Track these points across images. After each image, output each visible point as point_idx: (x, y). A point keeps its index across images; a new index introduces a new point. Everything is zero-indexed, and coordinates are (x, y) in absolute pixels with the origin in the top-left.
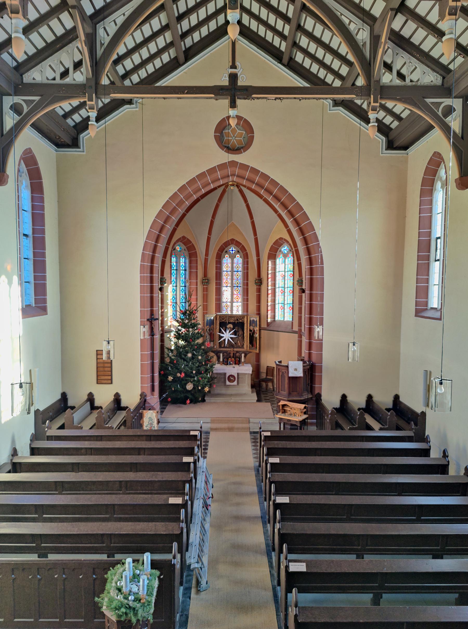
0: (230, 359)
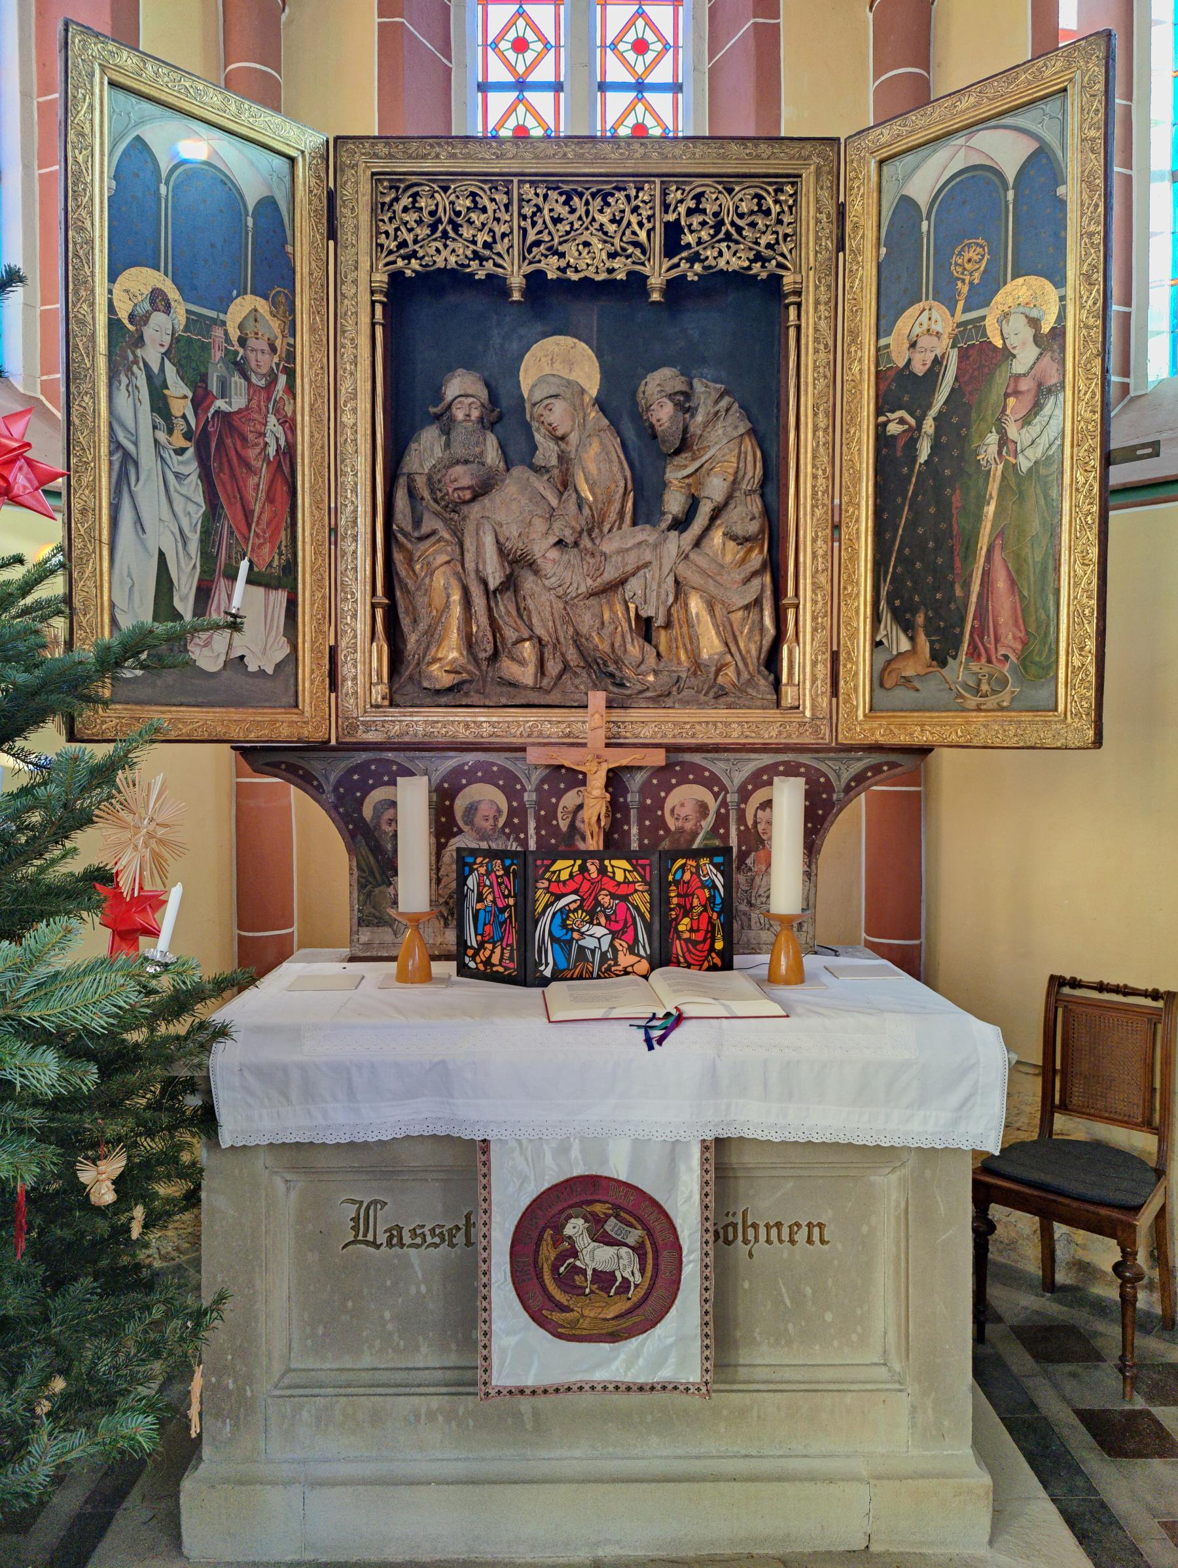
0: (564, 867)
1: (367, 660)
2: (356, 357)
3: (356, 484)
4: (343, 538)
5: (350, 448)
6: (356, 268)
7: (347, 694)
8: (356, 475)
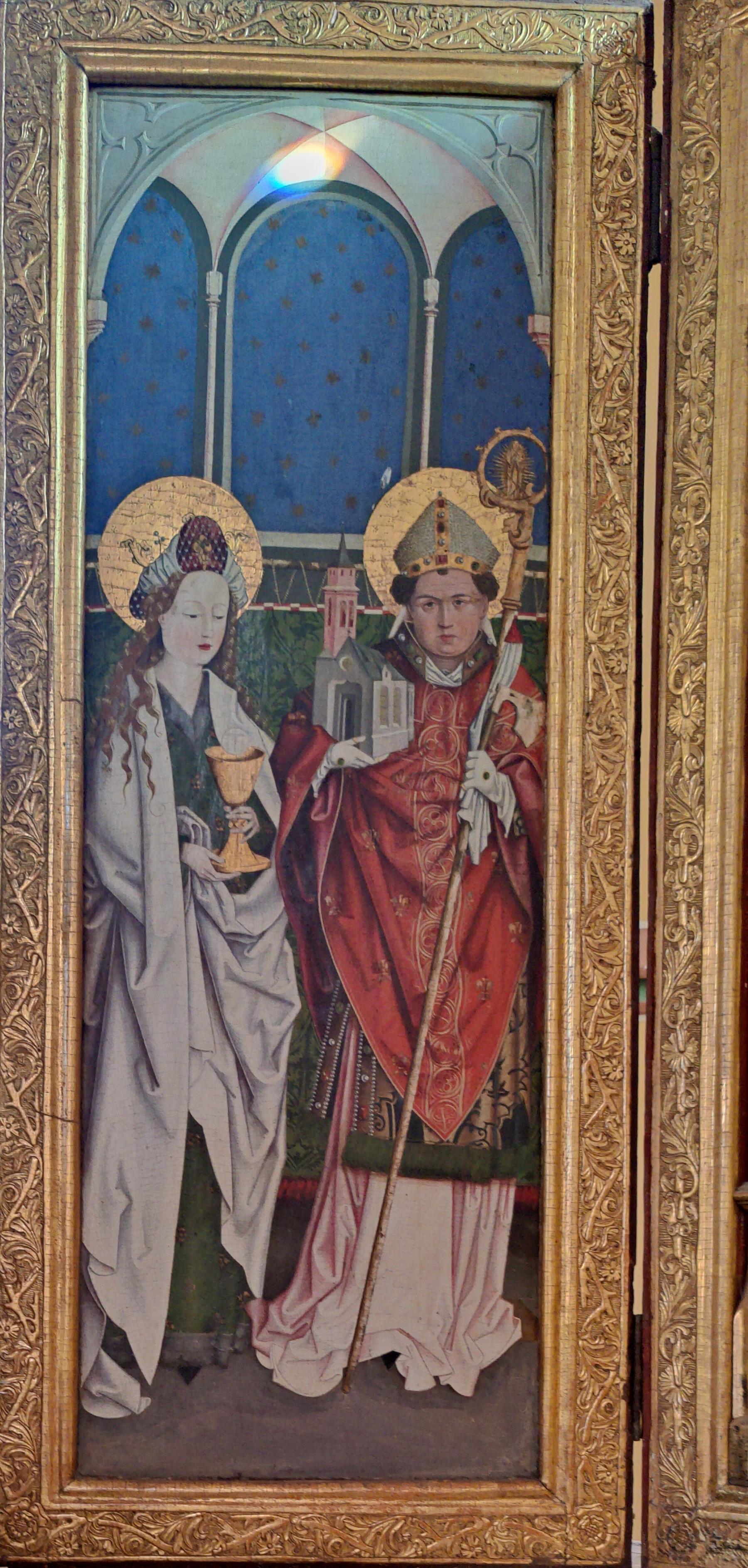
1: (722, 1357)
2: (706, 550)
3: (700, 887)
4: (669, 1031)
5: (689, 795)
6: (713, 313)
7: (671, 1445)
8: (699, 863)
